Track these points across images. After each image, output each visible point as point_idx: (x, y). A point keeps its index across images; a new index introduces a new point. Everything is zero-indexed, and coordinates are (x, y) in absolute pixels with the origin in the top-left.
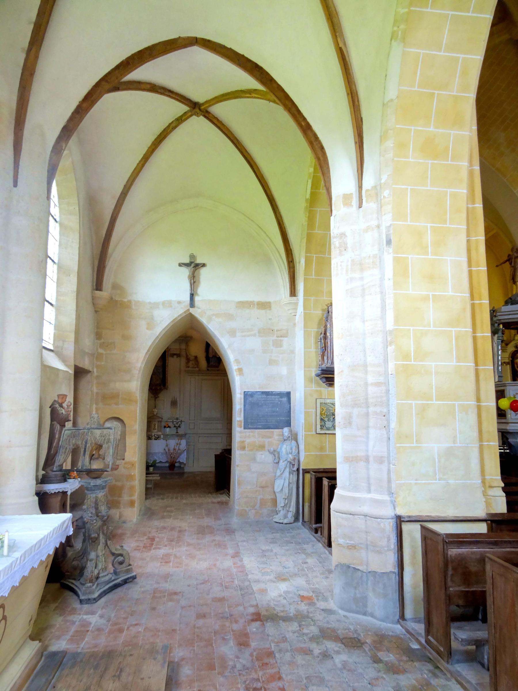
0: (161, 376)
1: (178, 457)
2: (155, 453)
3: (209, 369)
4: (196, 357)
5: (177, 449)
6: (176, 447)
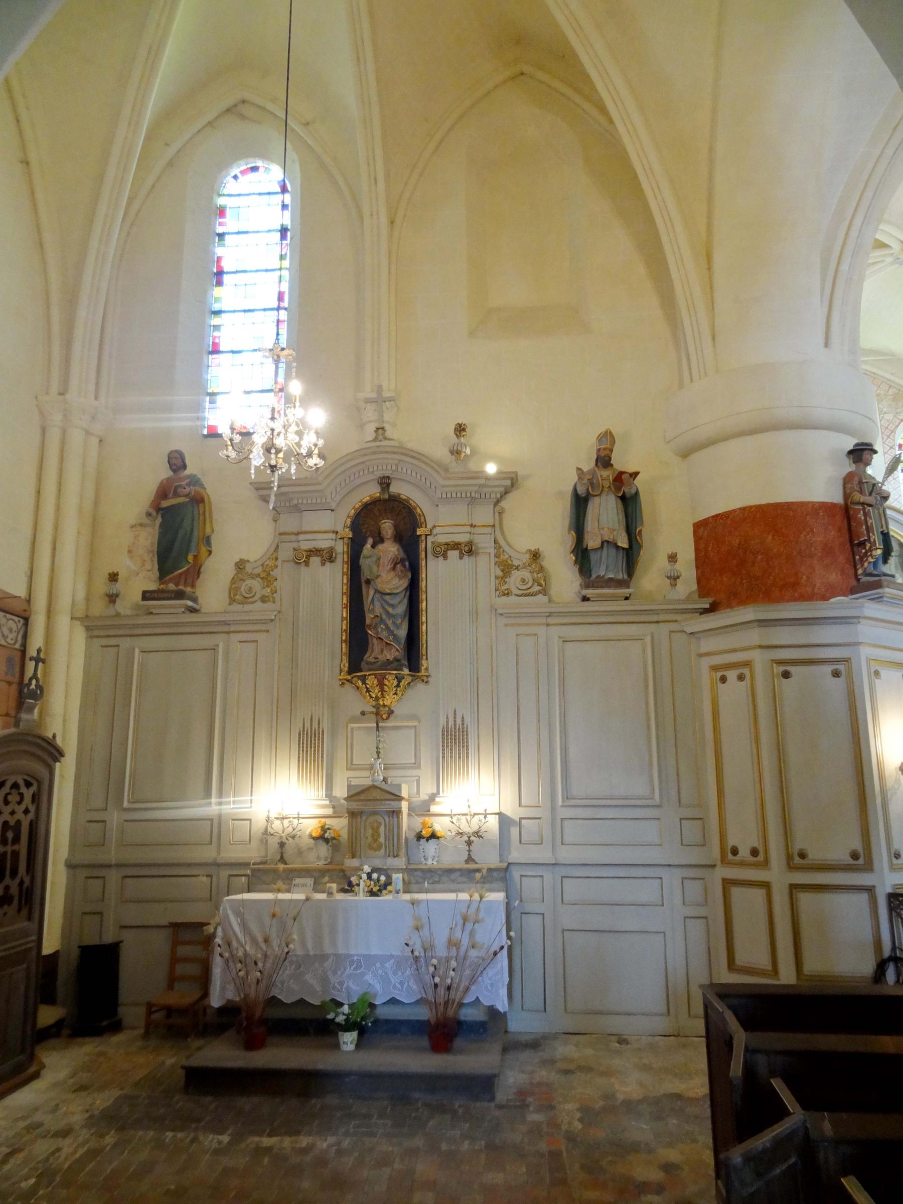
0: (403, 632)
1: (473, 980)
2: (367, 957)
3: (589, 592)
4: (535, 556)
5: (465, 942)
6: (458, 934)
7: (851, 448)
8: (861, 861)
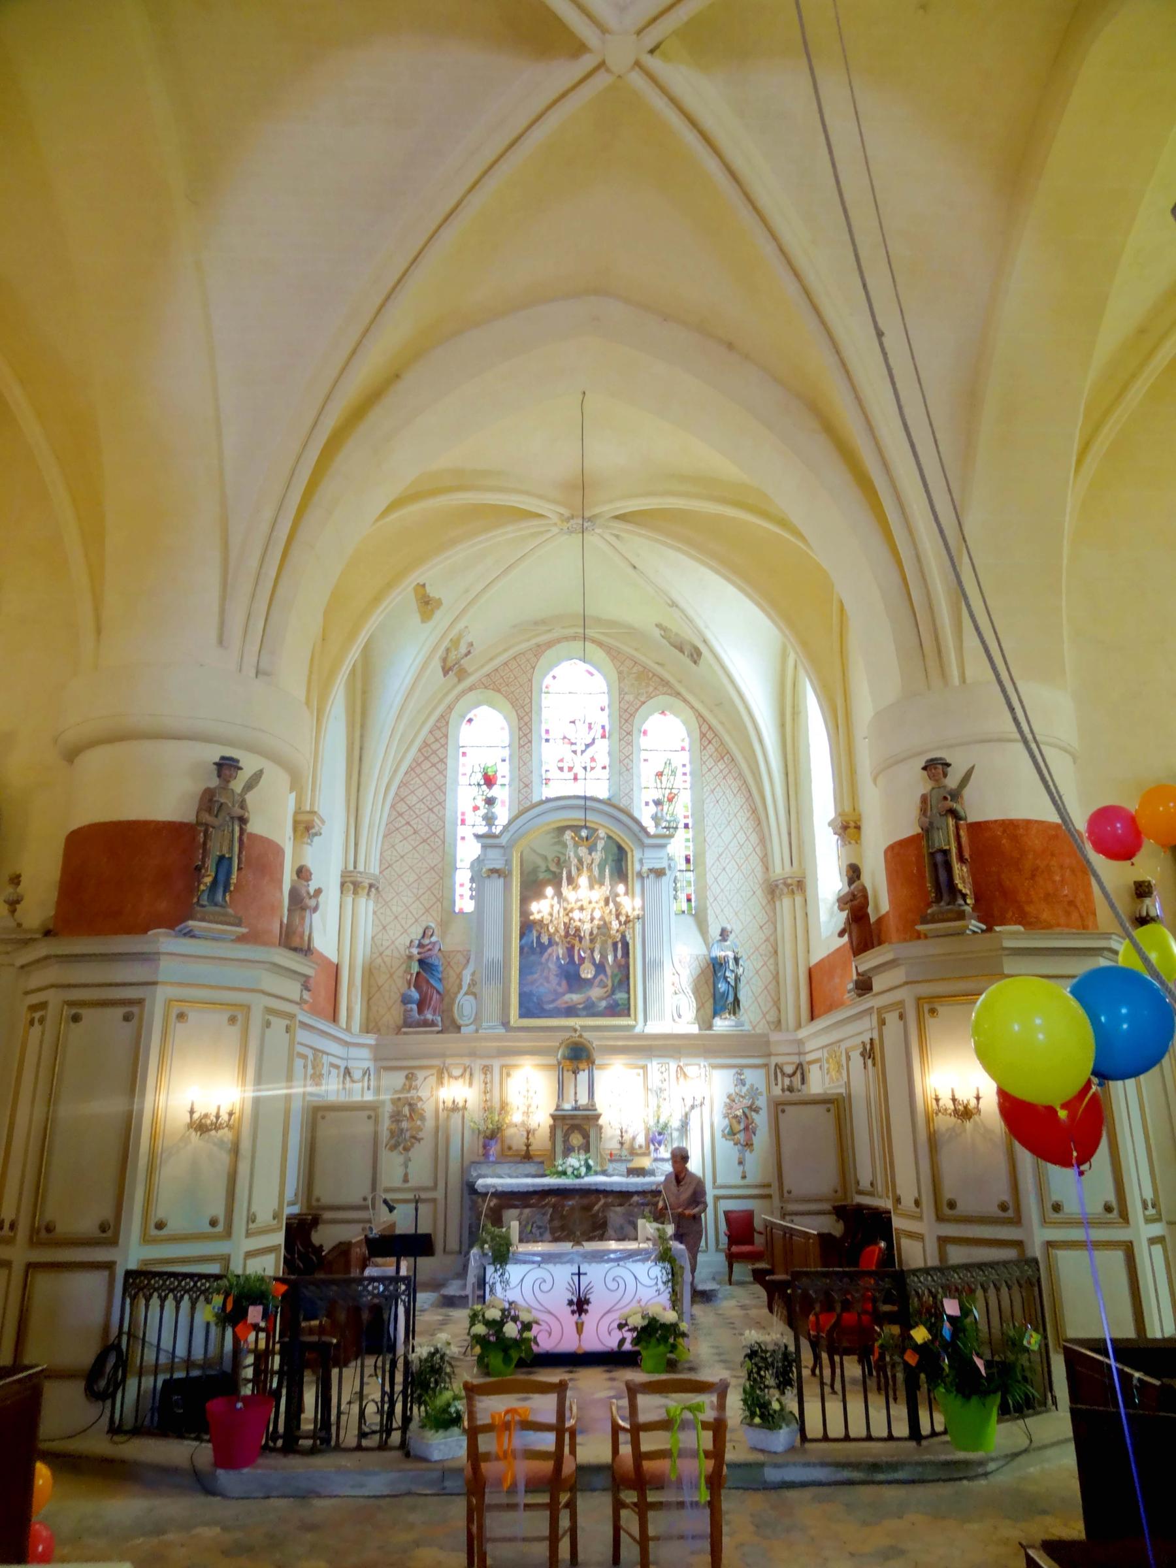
7: (217, 760)
8: (154, 1232)
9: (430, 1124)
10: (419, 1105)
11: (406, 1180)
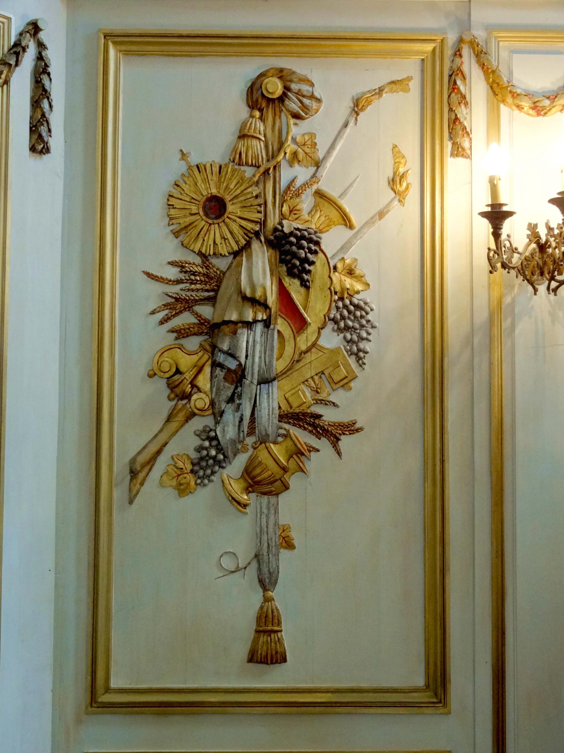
9: (394, 346)
10: (331, 241)
11: (266, 651)
